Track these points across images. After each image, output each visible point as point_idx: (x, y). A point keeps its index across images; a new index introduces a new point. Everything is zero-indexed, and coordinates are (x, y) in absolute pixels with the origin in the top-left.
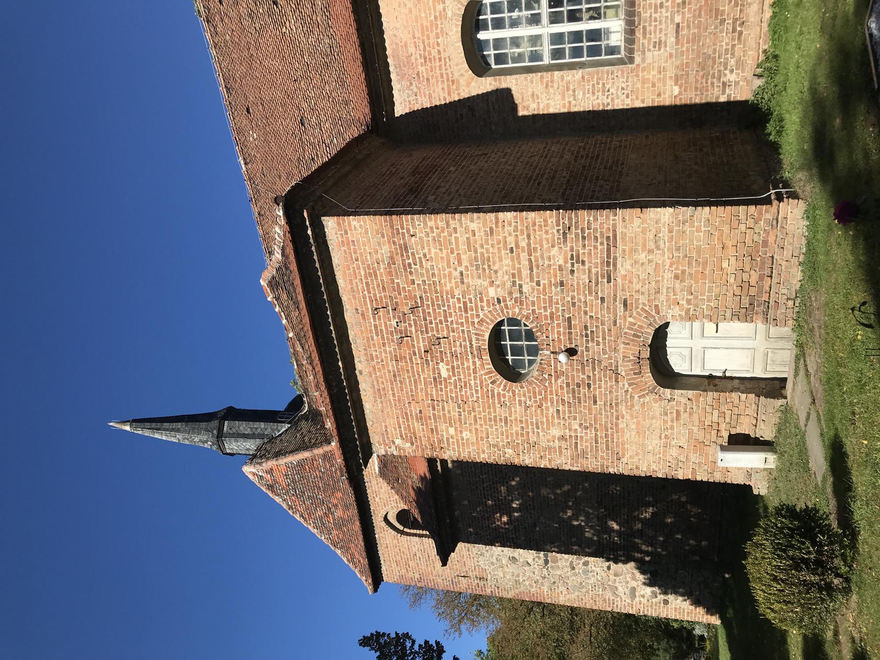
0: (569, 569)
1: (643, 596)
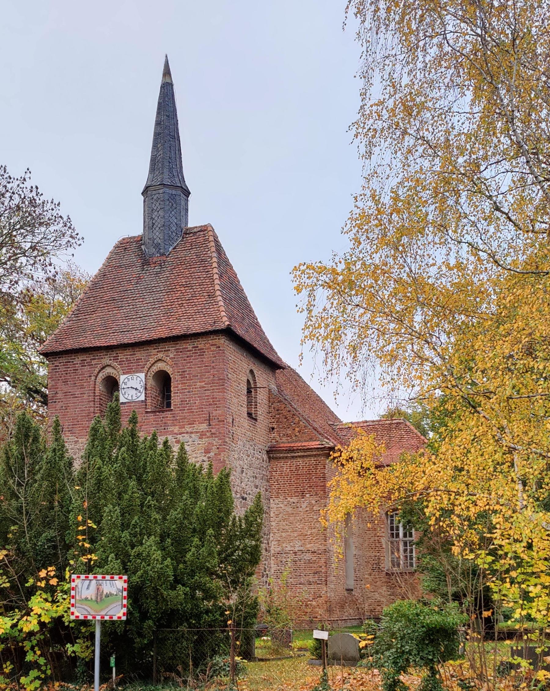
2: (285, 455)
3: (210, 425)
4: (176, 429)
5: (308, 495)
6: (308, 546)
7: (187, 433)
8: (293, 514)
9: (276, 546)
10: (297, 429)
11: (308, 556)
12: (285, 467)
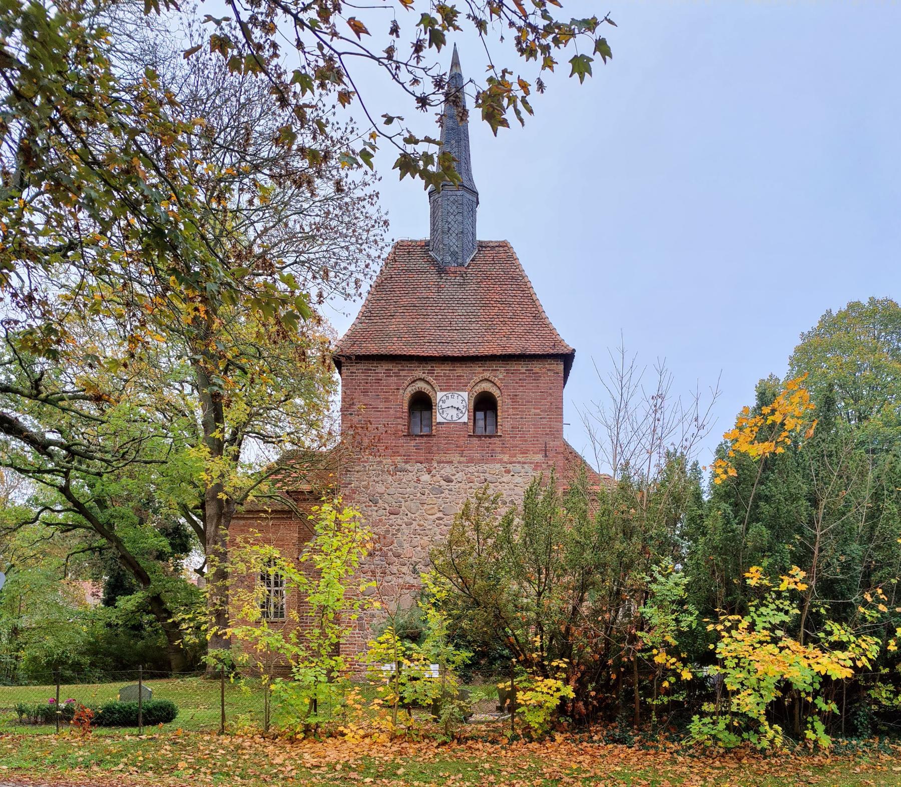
3: (546, 456)
4: (506, 458)
7: (519, 462)
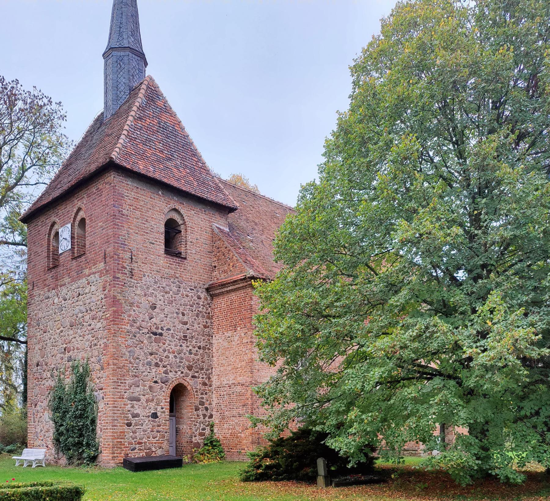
0: (150, 351)
1: (133, 407)
2: (221, 291)
5: (239, 329)
6: (239, 379)
8: (228, 348)
9: (217, 381)
10: (231, 264)
11: (239, 389)
12: (222, 302)
